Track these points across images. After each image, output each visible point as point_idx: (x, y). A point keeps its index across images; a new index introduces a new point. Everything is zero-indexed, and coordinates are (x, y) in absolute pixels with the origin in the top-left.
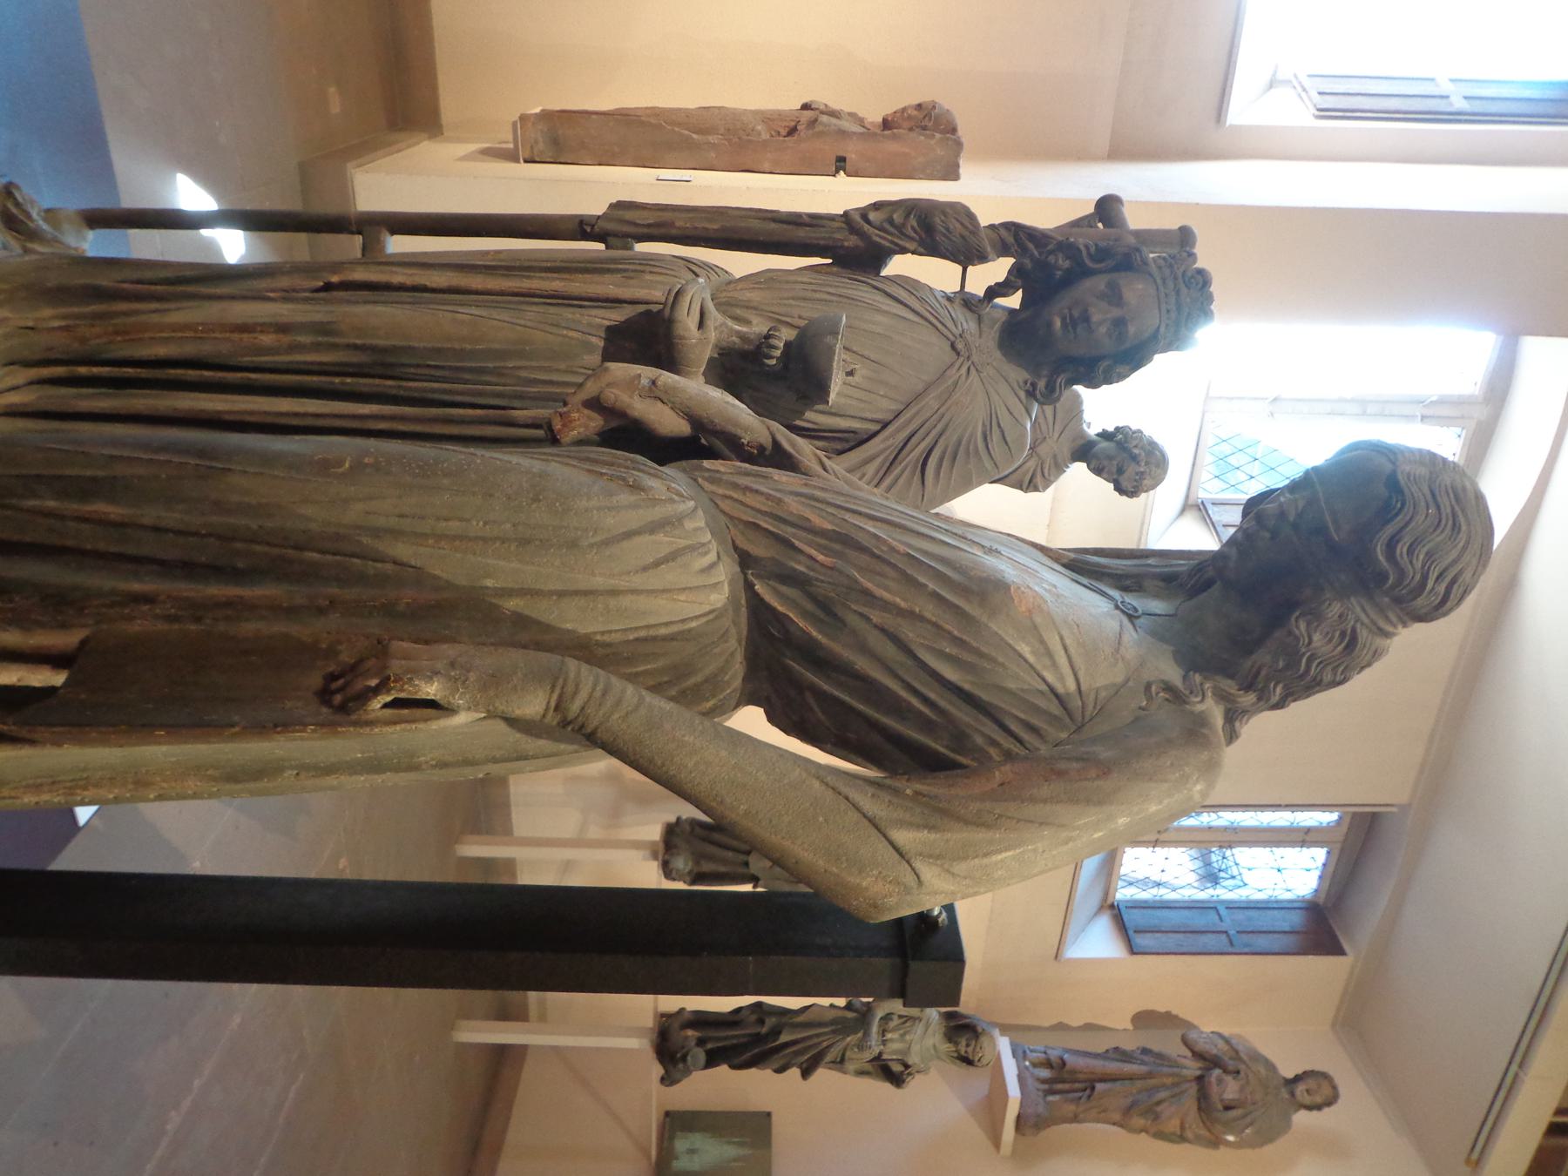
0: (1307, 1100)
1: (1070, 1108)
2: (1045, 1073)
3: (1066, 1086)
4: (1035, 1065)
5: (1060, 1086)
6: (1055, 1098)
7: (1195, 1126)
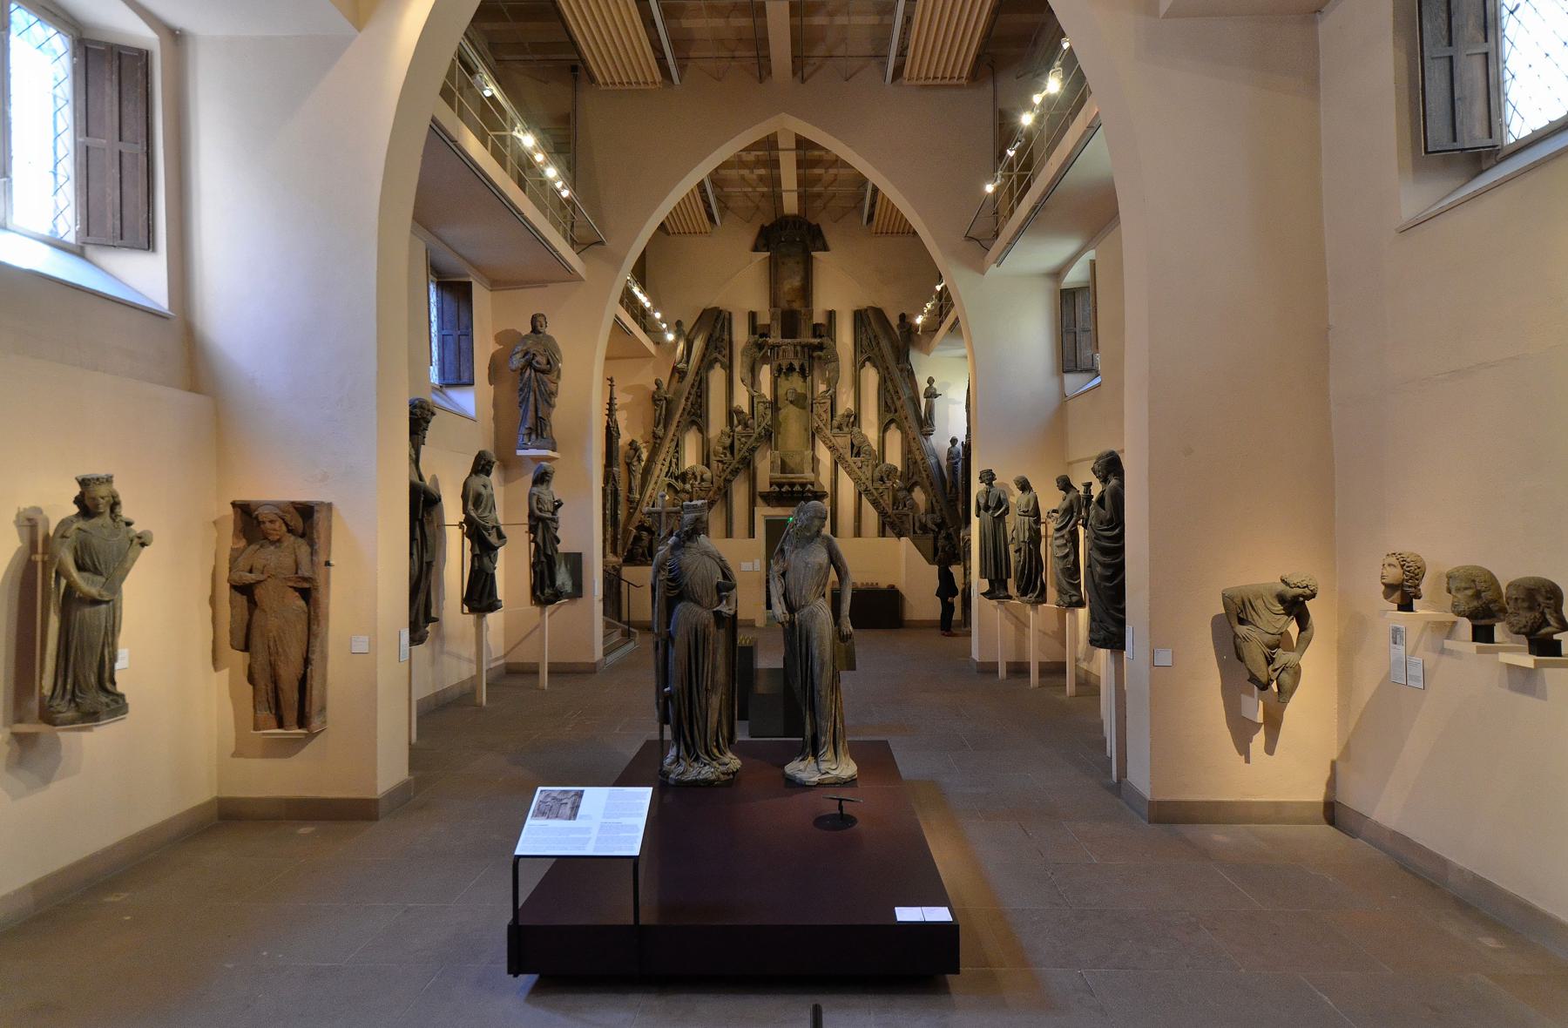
1: (548, 428)
2: (533, 437)
3: (539, 428)
4: (530, 440)
5: (539, 431)
6: (544, 434)
7: (553, 376)
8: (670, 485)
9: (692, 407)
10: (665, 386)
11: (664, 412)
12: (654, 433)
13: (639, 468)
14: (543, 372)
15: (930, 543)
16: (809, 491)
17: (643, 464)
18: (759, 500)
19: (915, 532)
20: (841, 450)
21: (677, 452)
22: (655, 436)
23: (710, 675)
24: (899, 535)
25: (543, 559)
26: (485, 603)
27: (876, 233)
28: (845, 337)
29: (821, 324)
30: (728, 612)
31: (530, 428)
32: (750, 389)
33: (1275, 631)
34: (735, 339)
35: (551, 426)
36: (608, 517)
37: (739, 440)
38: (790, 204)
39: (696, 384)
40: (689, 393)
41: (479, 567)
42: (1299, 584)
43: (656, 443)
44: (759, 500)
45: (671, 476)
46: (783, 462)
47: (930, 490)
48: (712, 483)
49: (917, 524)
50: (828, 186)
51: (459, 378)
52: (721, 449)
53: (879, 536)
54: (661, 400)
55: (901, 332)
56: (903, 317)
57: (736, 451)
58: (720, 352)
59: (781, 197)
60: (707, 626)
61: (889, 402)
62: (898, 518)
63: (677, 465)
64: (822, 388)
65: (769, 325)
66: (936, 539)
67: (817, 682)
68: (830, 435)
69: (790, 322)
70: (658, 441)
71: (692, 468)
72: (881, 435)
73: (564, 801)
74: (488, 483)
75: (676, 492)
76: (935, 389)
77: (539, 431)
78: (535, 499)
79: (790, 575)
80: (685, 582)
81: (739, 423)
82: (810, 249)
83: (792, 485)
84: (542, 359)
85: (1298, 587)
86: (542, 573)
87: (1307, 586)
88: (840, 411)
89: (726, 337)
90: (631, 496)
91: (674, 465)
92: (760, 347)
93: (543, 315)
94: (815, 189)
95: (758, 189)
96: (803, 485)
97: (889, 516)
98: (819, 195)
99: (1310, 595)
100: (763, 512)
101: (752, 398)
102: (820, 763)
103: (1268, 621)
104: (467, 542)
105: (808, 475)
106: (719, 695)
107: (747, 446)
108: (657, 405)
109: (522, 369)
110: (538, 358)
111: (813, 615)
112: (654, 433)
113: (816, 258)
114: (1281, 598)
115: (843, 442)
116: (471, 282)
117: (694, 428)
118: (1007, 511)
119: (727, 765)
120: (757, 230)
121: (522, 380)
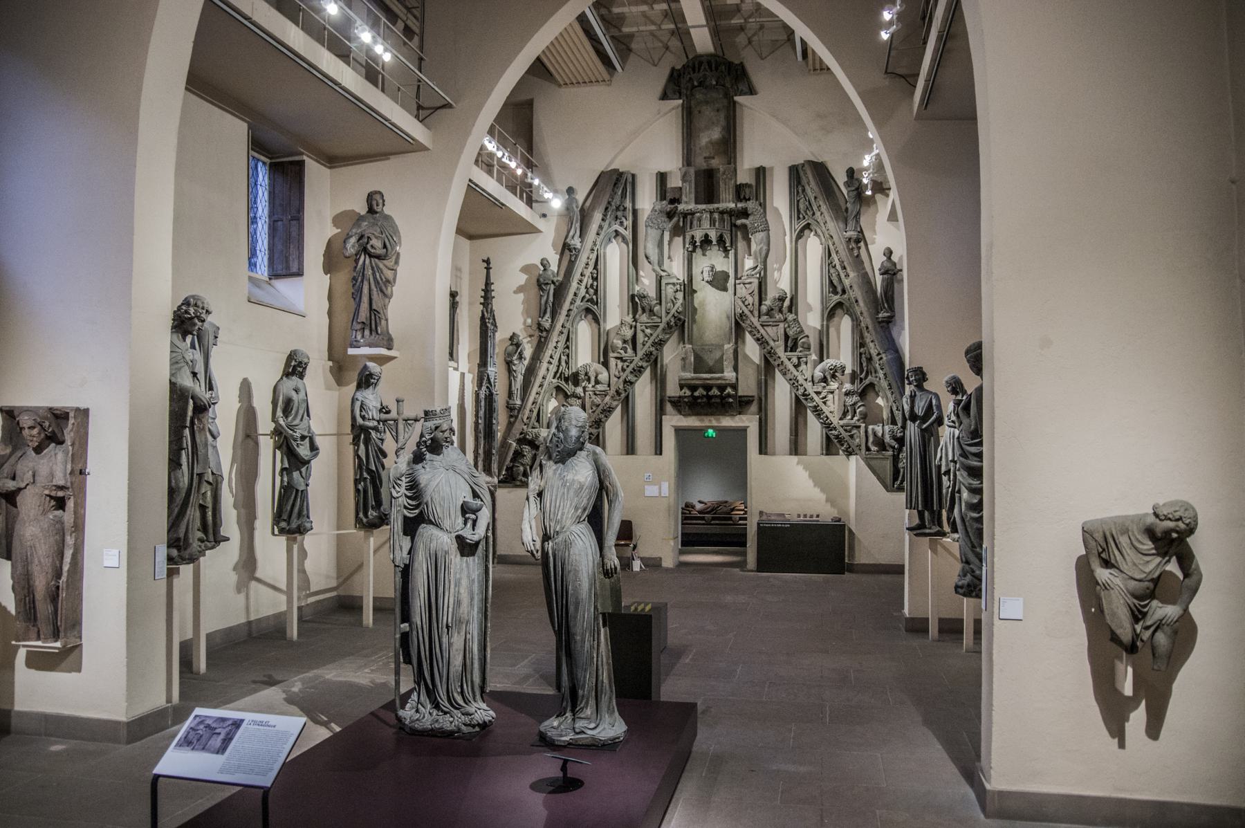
0: (381, 206)
1: (383, 322)
3: (373, 322)
5: (373, 326)
6: (379, 328)
7: (390, 263)
8: (558, 389)
9: (587, 292)
10: (554, 267)
11: (551, 299)
12: (539, 325)
13: (520, 368)
14: (379, 257)
15: (888, 465)
16: (729, 395)
17: (526, 362)
18: (669, 407)
19: (868, 449)
20: (772, 343)
21: (568, 347)
22: (540, 327)
23: (450, 610)
24: (849, 453)
25: (365, 475)
26: (294, 525)
27: (815, 70)
28: (779, 198)
29: (746, 184)
30: (469, 537)
31: (363, 323)
32: (657, 268)
33: (1142, 576)
34: (639, 206)
35: (387, 320)
36: (481, 427)
37: (643, 331)
38: (702, 40)
39: (592, 263)
40: (582, 275)
41: (288, 483)
42: (1171, 516)
43: (542, 336)
44: (669, 407)
45: (560, 377)
46: (698, 358)
47: (889, 395)
48: (609, 386)
49: (871, 439)
50: (750, 17)
51: (288, 268)
52: (619, 343)
54: (547, 284)
55: (848, 192)
56: (851, 173)
57: (639, 346)
58: (621, 223)
59: (689, 33)
60: (447, 552)
61: (835, 282)
62: (846, 430)
63: (567, 363)
64: (749, 263)
65: (681, 188)
66: (896, 459)
67: (571, 624)
68: (757, 324)
69: (707, 186)
70: (544, 334)
71: (585, 366)
72: (825, 323)
73: (217, 731)
74: (300, 386)
75: (566, 396)
76: (895, 264)
77: (373, 326)
78: (358, 404)
79: (547, 496)
80: (425, 501)
81: (644, 311)
82: (732, 94)
83: (708, 388)
84: (377, 243)
85: (1170, 519)
86: (365, 491)
87: (1180, 519)
88: (771, 294)
89: (628, 204)
90: (511, 402)
91: (563, 364)
92: (670, 215)
93: (380, 193)
94: (733, 22)
95: (664, 27)
96: (722, 388)
97: (835, 429)
98: (742, 28)
99: (1185, 530)
100: (673, 420)
101: (659, 280)
102: (577, 720)
103: (1135, 564)
104: (278, 453)
105: (729, 374)
106: (463, 633)
107: (652, 339)
108: (543, 290)
109: (356, 255)
110: (374, 242)
111: (568, 544)
112: (539, 325)
113: (741, 105)
114: (1150, 532)
115: (774, 333)
116: (303, 162)
117: (590, 317)
118: (940, 422)
119: (471, 715)
120: (667, 72)
121: (356, 267)
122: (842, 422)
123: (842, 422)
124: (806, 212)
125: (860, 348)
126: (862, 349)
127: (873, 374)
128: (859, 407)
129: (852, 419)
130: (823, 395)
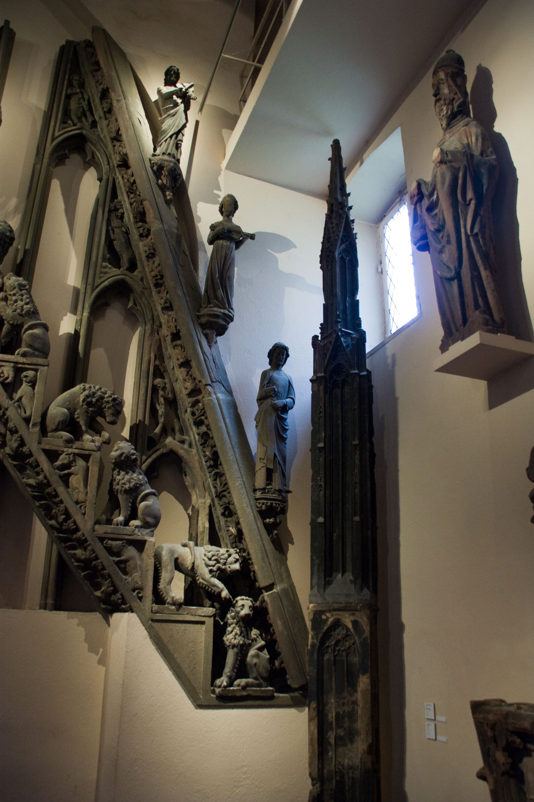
53: (44, 607)
61: (117, 245)
62: (110, 550)
97: (82, 543)
122: (101, 529)
123: (101, 529)
124: (80, 119)
125: (155, 376)
126: (158, 381)
127: (178, 436)
128: (144, 498)
129: (126, 523)
130: (63, 459)
